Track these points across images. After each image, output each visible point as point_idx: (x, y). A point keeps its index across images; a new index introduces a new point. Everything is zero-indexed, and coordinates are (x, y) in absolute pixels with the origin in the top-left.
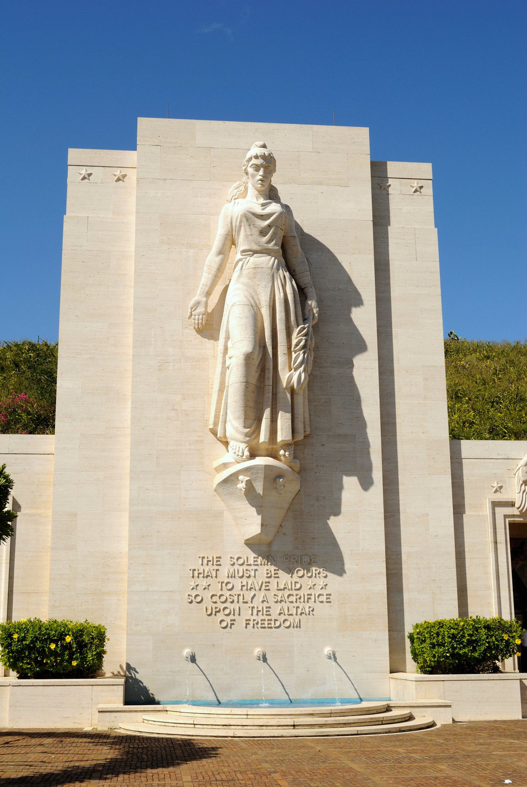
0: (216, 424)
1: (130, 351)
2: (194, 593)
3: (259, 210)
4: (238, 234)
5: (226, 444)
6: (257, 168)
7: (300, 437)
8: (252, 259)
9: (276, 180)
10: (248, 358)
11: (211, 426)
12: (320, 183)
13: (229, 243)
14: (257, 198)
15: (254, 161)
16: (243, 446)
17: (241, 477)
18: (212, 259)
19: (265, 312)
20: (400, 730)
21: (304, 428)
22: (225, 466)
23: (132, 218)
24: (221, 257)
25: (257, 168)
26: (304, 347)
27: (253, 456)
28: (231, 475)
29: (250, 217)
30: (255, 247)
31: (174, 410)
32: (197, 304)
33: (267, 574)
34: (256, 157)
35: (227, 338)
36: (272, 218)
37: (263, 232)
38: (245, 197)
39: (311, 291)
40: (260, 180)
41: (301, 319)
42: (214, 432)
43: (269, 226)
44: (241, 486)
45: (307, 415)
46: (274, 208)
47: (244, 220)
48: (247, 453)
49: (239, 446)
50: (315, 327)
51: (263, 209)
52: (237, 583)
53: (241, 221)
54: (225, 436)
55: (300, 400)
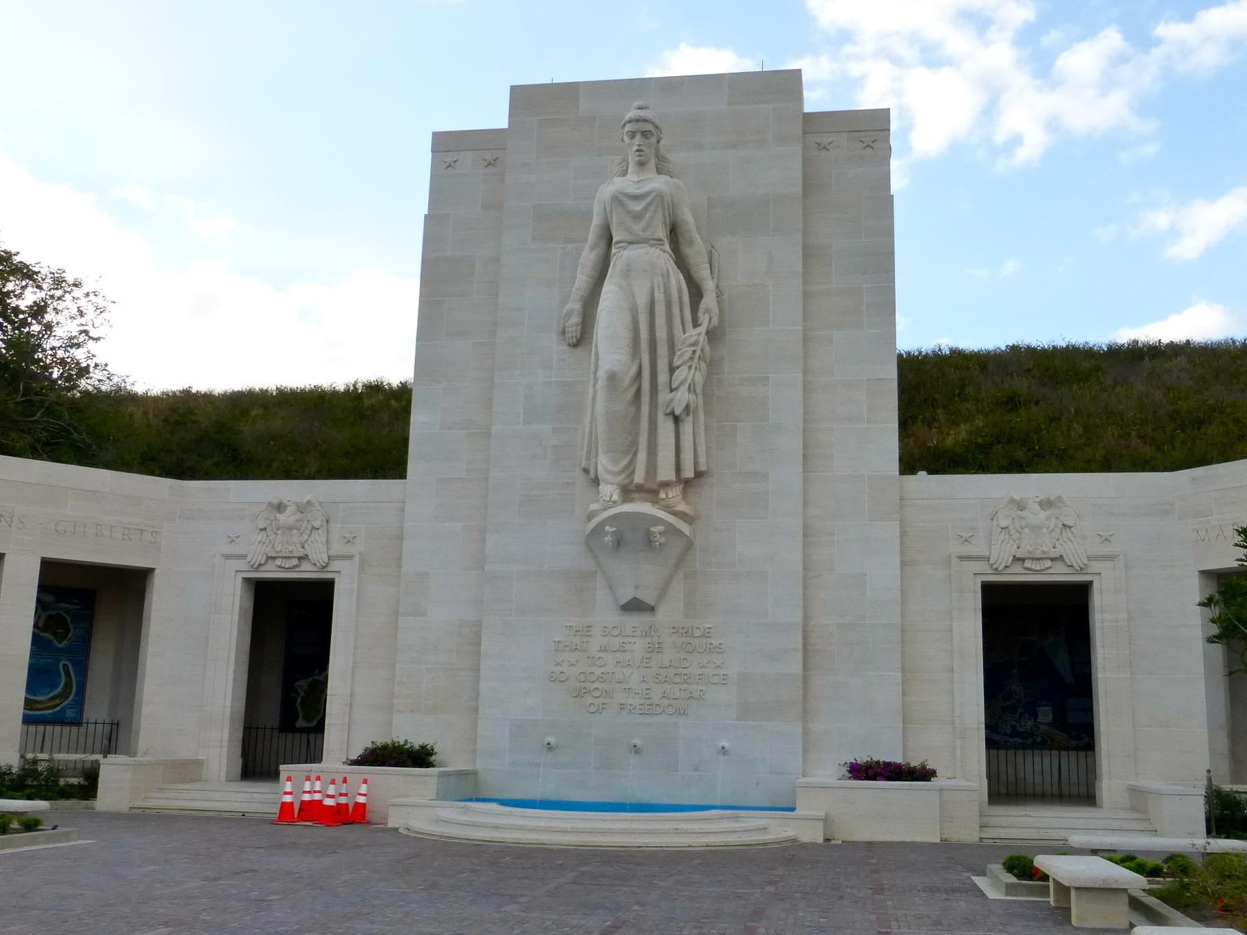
2: (559, 669)
3: (632, 190)
6: (632, 135)
7: (689, 473)
8: (626, 252)
15: (627, 128)
21: (696, 463)
25: (632, 135)
29: (618, 200)
30: (629, 238)
36: (649, 199)
37: (637, 217)
39: (709, 286)
41: (689, 324)
42: (586, 471)
43: (646, 208)
44: (608, 539)
46: (658, 183)
48: (615, 497)
49: (609, 490)
52: (609, 658)
55: (687, 427)
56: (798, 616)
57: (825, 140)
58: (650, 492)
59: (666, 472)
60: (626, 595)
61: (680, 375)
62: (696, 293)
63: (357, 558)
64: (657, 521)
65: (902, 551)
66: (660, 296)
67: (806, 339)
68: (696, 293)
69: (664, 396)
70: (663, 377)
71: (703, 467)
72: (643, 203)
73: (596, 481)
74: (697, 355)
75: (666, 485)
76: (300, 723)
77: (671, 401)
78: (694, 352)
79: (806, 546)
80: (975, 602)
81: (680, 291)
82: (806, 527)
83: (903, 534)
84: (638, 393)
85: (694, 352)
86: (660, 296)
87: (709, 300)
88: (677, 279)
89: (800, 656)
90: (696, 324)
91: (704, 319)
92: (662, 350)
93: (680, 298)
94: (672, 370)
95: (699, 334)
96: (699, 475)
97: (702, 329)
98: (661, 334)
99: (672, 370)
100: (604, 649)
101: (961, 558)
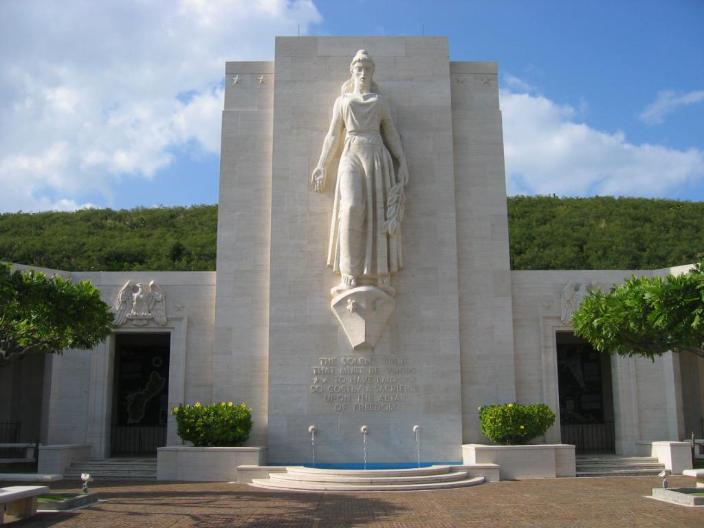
0: (332, 261)
1: (270, 209)
4: (347, 119)
5: (340, 275)
9: (375, 78)
10: (353, 211)
11: (328, 263)
12: (411, 79)
13: (340, 126)
14: (361, 93)
15: (357, 65)
16: (350, 277)
17: (349, 301)
18: (328, 138)
20: (452, 487)
21: (398, 263)
22: (339, 292)
23: (272, 111)
24: (333, 138)
26: (397, 202)
27: (358, 284)
28: (342, 299)
29: (354, 105)
31: (302, 251)
32: (318, 173)
33: (371, 372)
34: (359, 61)
35: (340, 198)
36: (372, 106)
38: (352, 91)
40: (362, 78)
41: (394, 181)
43: (369, 112)
44: (350, 307)
45: (400, 254)
47: (350, 108)
50: (406, 188)
51: (365, 100)
53: (348, 110)
54: (339, 271)
55: (393, 242)
56: (458, 352)
59: (382, 268)
61: (391, 211)
62: (396, 161)
63: (185, 321)
65: (514, 312)
67: (457, 191)
68: (396, 161)
69: (380, 222)
70: (380, 212)
71: (401, 264)
72: (367, 110)
74: (400, 198)
75: (384, 276)
76: (130, 421)
77: (387, 225)
78: (398, 198)
79: (460, 310)
80: (552, 342)
81: (389, 161)
82: (460, 299)
83: (513, 304)
84: (366, 221)
85: (398, 198)
87: (403, 168)
89: (459, 375)
90: (397, 182)
92: (380, 196)
93: (389, 165)
95: (400, 187)
96: (400, 269)
97: (401, 185)
98: (379, 185)
100: (344, 373)
101: (545, 318)
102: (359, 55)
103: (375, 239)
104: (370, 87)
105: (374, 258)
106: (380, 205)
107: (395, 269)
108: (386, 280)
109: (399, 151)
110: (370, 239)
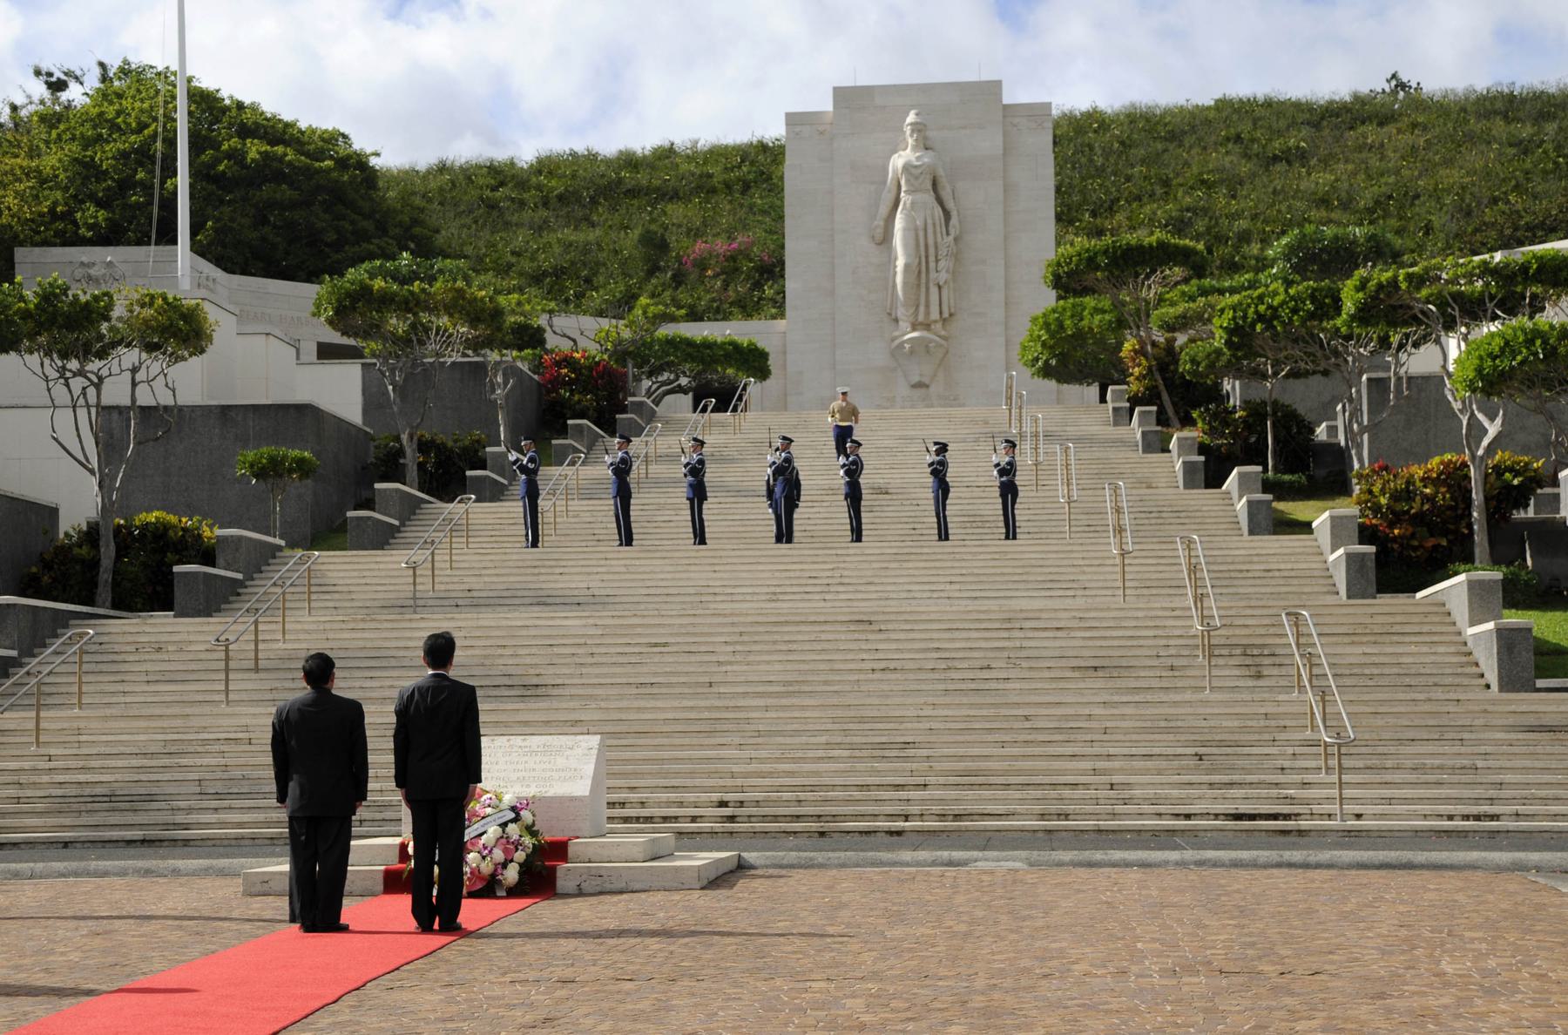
7: (946, 315)
19: (921, 234)
39: (954, 214)
50: (956, 239)
57: (1016, 120)
58: (927, 326)
59: (935, 315)
60: (916, 379)
61: (942, 264)
62: (947, 214)
64: (931, 341)
66: (930, 221)
67: (1006, 238)
68: (947, 214)
69: (933, 275)
70: (932, 265)
73: (896, 320)
86: (930, 221)
87: (954, 221)
88: (938, 211)
91: (952, 231)
92: (932, 251)
94: (937, 261)
97: (951, 238)
98: (931, 242)
99: (937, 261)
102: (911, 117)
103: (927, 289)
104: (925, 145)
105: (927, 306)
106: (932, 258)
107: (946, 315)
108: (939, 325)
109: (950, 205)
110: (923, 289)
